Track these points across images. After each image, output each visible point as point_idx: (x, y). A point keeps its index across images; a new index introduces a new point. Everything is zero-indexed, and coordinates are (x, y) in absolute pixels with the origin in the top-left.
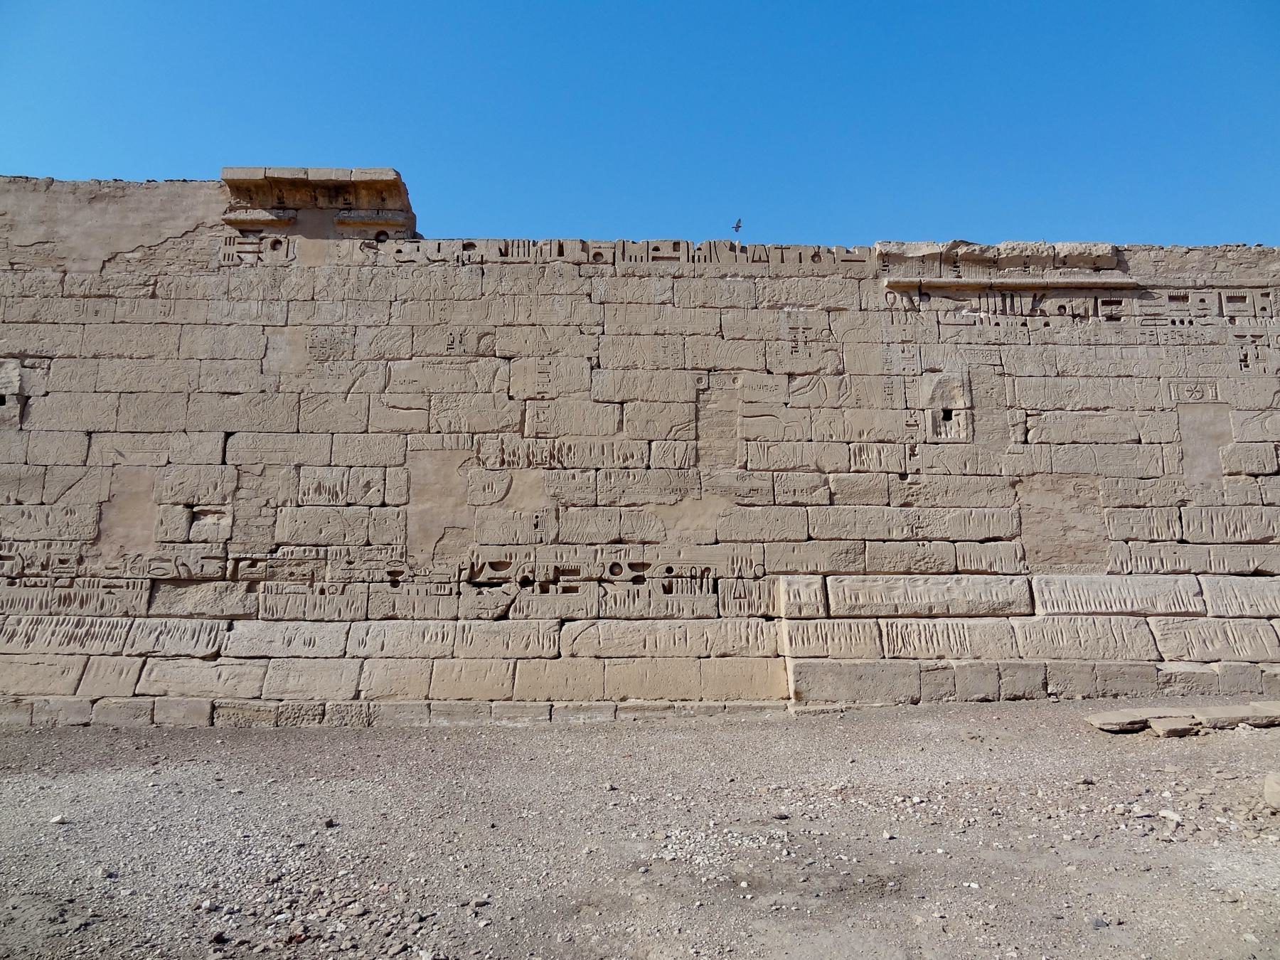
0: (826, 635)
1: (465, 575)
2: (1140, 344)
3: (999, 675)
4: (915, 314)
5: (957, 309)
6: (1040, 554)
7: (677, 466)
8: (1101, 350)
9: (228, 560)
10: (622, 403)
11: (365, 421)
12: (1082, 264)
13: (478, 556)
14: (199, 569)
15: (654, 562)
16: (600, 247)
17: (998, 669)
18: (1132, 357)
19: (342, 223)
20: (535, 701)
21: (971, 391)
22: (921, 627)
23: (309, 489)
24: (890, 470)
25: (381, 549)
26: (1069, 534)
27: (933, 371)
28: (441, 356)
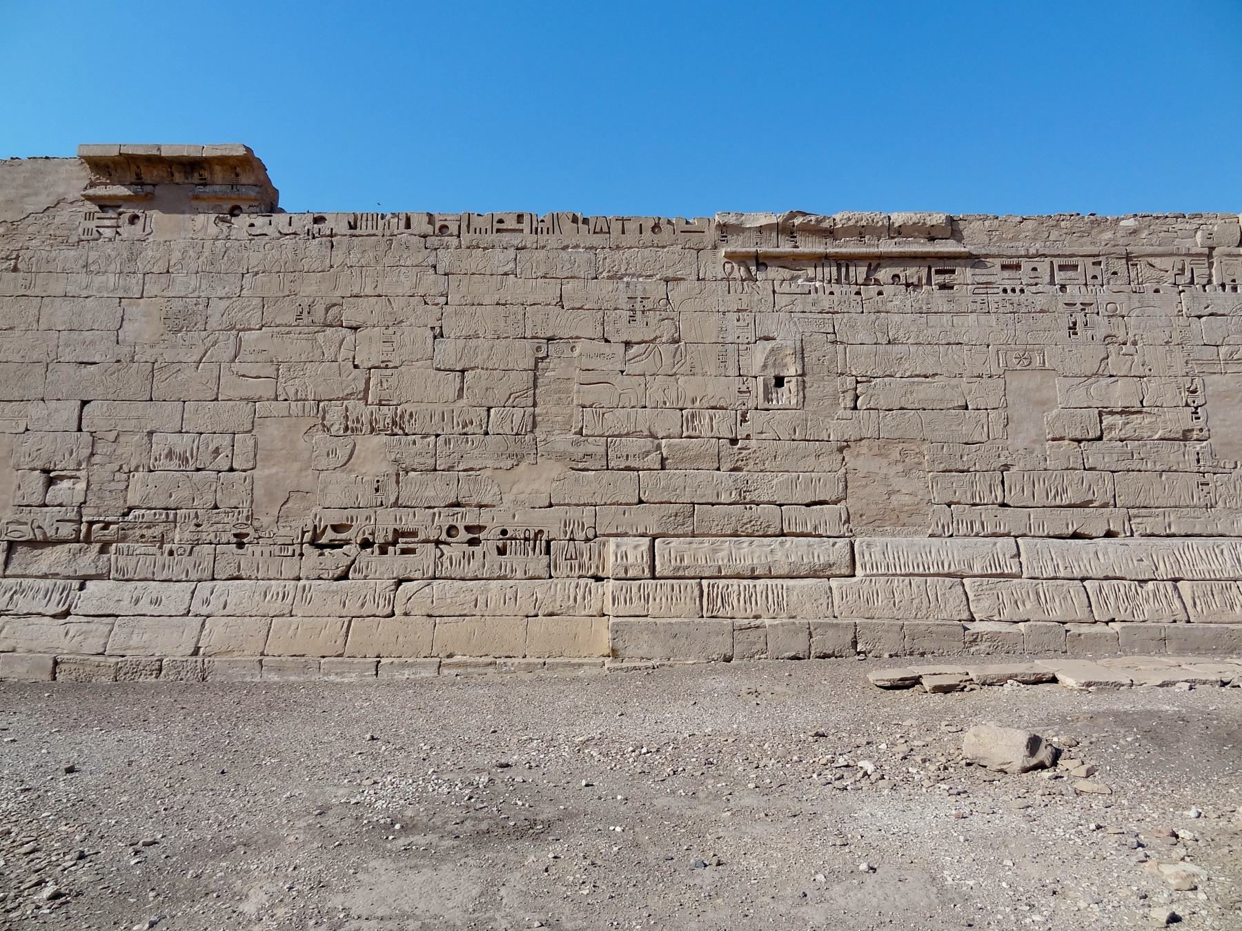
0: (648, 595)
1: (308, 537)
2: (971, 312)
3: (810, 634)
4: (751, 283)
5: (793, 278)
6: (864, 517)
7: (515, 431)
8: (932, 317)
9: (82, 523)
10: (463, 371)
11: (216, 389)
12: (916, 234)
13: (320, 519)
14: (53, 532)
15: (489, 525)
16: (446, 220)
17: (809, 628)
18: (963, 324)
19: (197, 198)
20: (365, 657)
21: (803, 358)
22: (742, 588)
23: (160, 455)
24: (721, 436)
25: (228, 512)
26: (893, 497)
27: (767, 339)
28: (290, 326)
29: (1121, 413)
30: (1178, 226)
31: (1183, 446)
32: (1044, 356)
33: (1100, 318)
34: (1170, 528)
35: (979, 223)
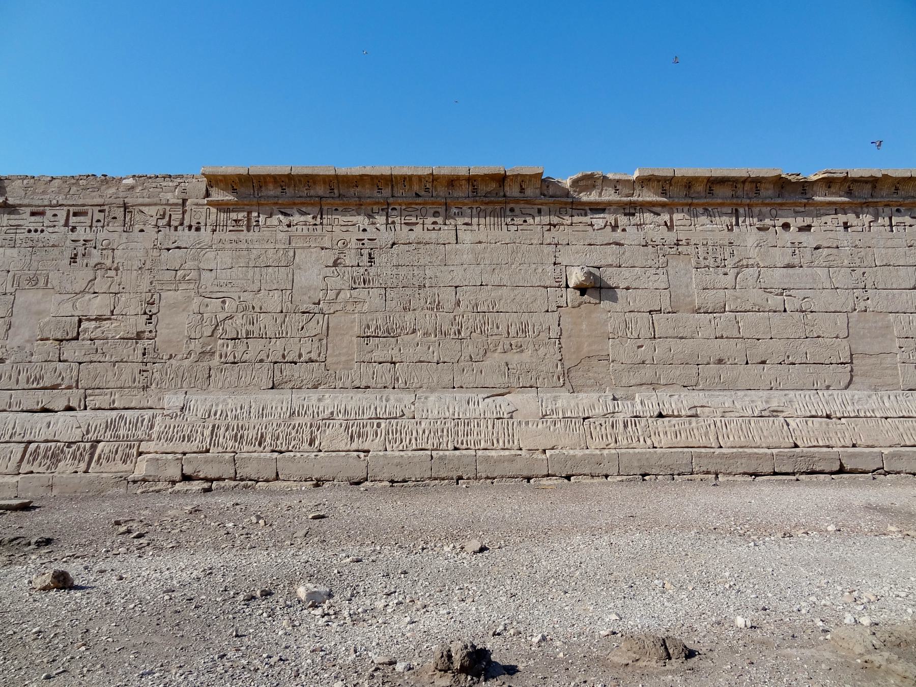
29: (96, 320)
30: (164, 184)
31: (135, 343)
32: (48, 278)
33: (94, 251)
34: (113, 404)
35: (19, 181)
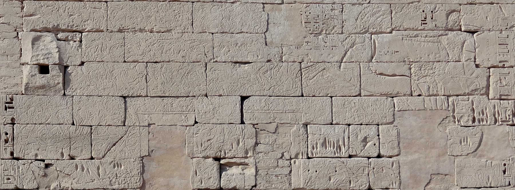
23: (317, 144)
28: (417, 30)
